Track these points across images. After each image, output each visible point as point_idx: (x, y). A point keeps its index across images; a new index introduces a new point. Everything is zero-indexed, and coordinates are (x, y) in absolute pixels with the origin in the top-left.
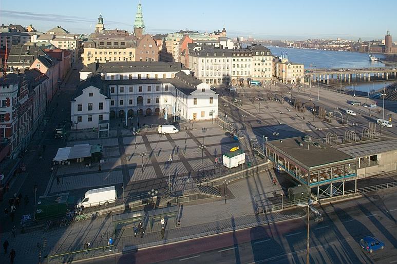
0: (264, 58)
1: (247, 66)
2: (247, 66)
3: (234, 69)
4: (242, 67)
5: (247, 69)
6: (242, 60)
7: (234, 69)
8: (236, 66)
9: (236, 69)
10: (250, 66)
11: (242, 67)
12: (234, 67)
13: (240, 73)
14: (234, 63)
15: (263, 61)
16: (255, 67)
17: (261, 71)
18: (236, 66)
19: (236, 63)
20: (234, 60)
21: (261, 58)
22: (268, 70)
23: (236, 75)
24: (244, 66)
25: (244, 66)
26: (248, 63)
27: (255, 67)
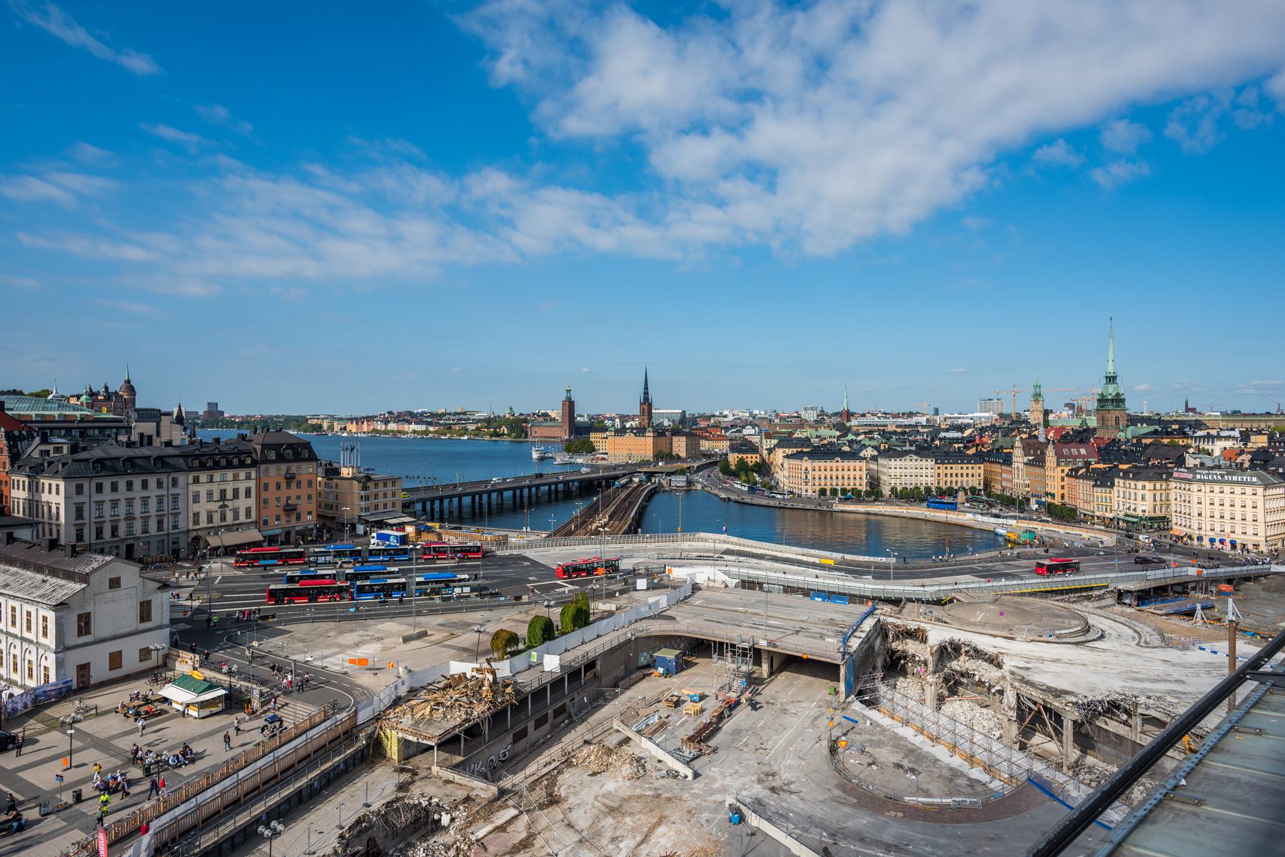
0: (294, 467)
1: (242, 493)
2: (242, 493)
3: (195, 508)
7: (195, 508)
8: (203, 497)
9: (203, 507)
12: (196, 499)
13: (216, 517)
14: (194, 488)
15: (290, 478)
16: (264, 495)
18: (203, 497)
19: (203, 490)
20: (196, 480)
21: (284, 467)
23: (203, 523)
24: (229, 495)
25: (229, 495)
27: (264, 495)
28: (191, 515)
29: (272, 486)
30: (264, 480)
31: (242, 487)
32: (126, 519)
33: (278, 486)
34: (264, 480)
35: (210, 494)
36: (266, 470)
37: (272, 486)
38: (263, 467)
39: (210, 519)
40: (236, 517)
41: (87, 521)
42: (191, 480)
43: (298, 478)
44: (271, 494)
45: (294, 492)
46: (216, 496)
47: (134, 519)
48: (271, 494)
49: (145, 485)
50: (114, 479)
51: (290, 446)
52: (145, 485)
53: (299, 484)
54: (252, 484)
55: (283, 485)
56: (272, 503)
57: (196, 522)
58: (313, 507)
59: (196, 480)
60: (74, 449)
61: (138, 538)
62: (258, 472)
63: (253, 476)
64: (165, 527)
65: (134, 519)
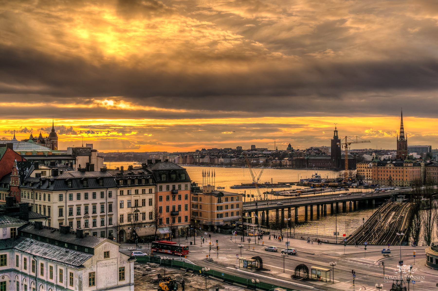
3: (120, 211)
4: (136, 205)
5: (148, 209)
6: (137, 192)
7: (120, 211)
9: (125, 211)
10: (150, 204)
11: (136, 205)
16: (160, 204)
17: (171, 209)
19: (125, 199)
20: (122, 193)
22: (183, 208)
23: (126, 222)
24: (140, 204)
25: (140, 204)
26: (147, 197)
27: (160, 204)
28: (119, 216)
29: (164, 198)
30: (160, 194)
31: (147, 197)
32: (84, 218)
33: (168, 198)
34: (160, 194)
35: (129, 203)
36: (161, 188)
37: (164, 198)
38: (159, 185)
39: (129, 220)
40: (144, 218)
41: (64, 218)
42: (119, 194)
43: (180, 193)
44: (163, 204)
45: (177, 203)
46: (133, 204)
47: (89, 217)
48: (163, 204)
49: (94, 196)
50: (86, 191)
51: (175, 171)
52: (94, 196)
53: (180, 198)
54: (152, 196)
55: (171, 198)
56: (164, 210)
57: (122, 220)
58: (188, 213)
59: (122, 193)
60: (55, 173)
61: (90, 230)
62: (156, 189)
63: (153, 191)
64: (105, 223)
65: (89, 217)
